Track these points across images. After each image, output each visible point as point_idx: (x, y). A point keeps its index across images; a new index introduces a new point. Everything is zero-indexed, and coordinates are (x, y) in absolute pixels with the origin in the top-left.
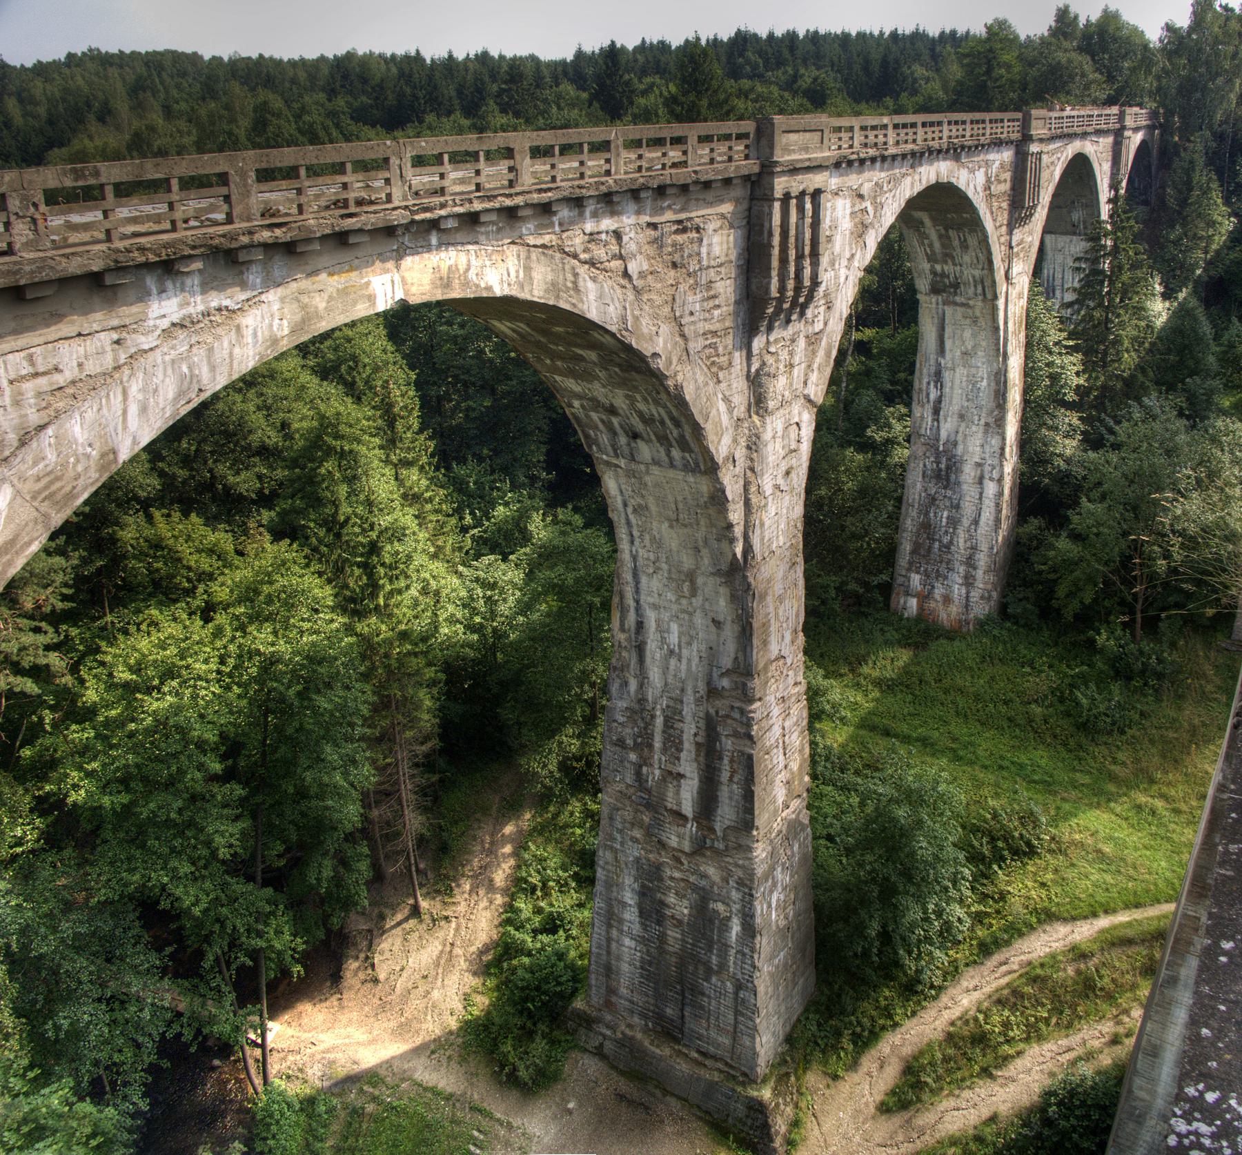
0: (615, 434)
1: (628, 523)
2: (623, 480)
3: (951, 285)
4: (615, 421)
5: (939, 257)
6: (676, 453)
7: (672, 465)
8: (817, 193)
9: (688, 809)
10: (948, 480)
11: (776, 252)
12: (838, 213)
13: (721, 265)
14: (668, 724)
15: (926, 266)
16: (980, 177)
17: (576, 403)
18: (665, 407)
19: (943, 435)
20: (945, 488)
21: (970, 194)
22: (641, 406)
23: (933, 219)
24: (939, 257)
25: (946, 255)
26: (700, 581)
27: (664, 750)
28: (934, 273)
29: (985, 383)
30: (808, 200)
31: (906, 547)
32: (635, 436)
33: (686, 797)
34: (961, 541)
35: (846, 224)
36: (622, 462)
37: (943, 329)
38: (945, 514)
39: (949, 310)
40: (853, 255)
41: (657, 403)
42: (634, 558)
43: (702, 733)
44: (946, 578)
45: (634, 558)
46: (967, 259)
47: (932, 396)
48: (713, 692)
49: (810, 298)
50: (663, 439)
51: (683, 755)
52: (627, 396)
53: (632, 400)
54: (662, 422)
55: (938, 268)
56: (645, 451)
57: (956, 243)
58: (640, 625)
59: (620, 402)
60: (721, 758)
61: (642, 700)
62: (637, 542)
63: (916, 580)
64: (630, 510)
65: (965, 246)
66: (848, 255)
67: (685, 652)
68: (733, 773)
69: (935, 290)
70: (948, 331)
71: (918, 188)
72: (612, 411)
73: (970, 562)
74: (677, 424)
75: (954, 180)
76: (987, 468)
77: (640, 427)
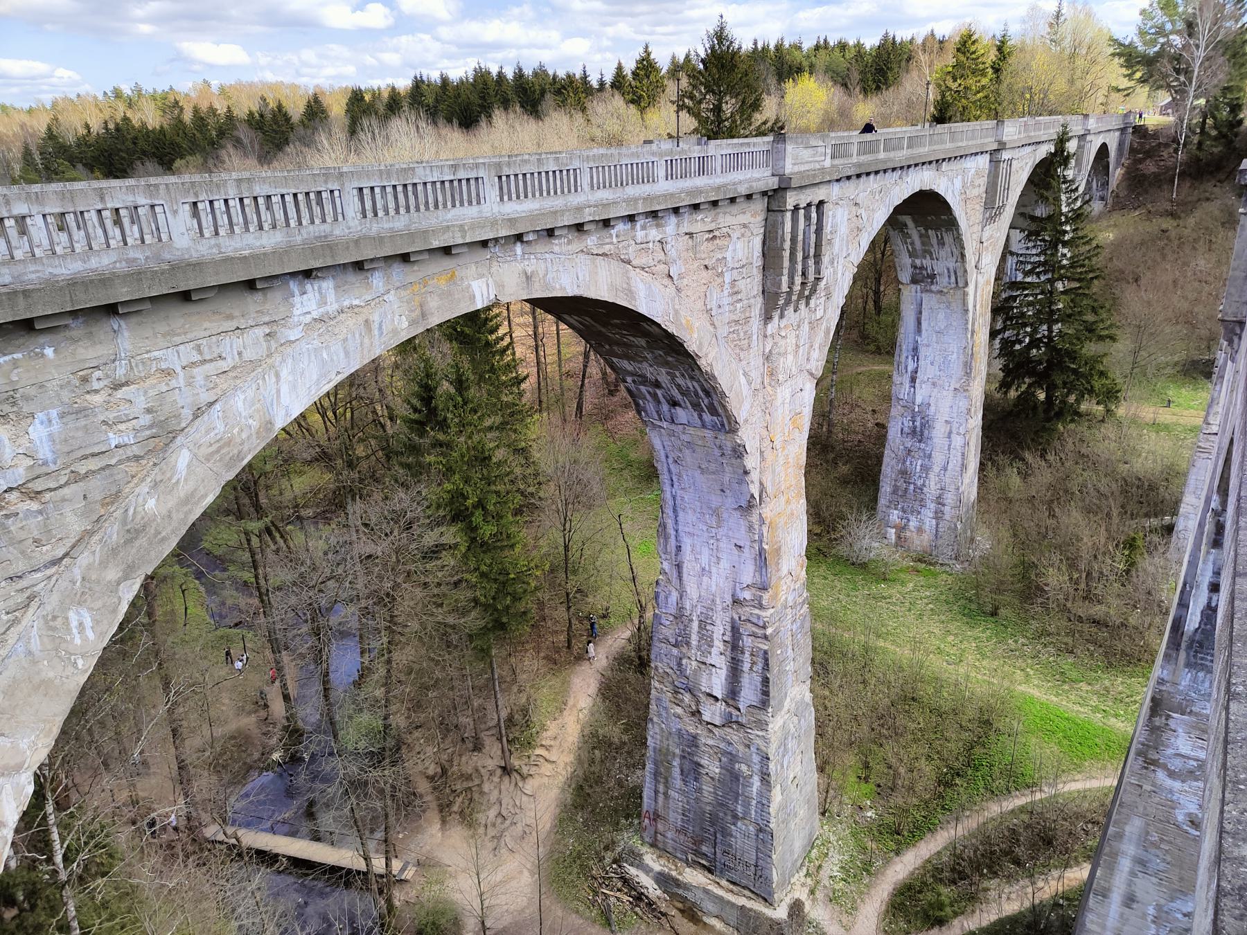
0: (659, 402)
1: (669, 471)
2: (666, 438)
3: (929, 276)
4: (659, 392)
5: (919, 253)
6: (707, 417)
7: (704, 426)
9: (718, 693)
10: (922, 435)
12: (838, 220)
14: (702, 624)
15: (906, 260)
17: (629, 379)
18: (698, 381)
19: (918, 400)
20: (920, 441)
22: (680, 381)
23: (914, 221)
24: (919, 253)
25: (925, 251)
26: (725, 515)
27: (699, 648)
29: (955, 356)
31: (886, 488)
32: (674, 404)
33: (717, 683)
34: (932, 483)
35: (843, 229)
36: (665, 425)
38: (919, 462)
41: (692, 378)
42: (674, 498)
43: (729, 633)
44: (919, 513)
45: (674, 498)
46: (943, 253)
47: (910, 368)
48: (736, 602)
49: (814, 291)
50: (696, 406)
51: (714, 651)
52: (668, 373)
53: (673, 377)
54: (696, 394)
55: (918, 262)
56: (682, 414)
58: (679, 548)
59: (664, 378)
60: (743, 653)
61: (681, 609)
62: (676, 484)
63: (895, 515)
64: (670, 460)
67: (714, 570)
68: (753, 663)
69: (914, 281)
72: (657, 385)
73: (939, 501)
74: (708, 394)
76: (955, 425)
77: (679, 397)
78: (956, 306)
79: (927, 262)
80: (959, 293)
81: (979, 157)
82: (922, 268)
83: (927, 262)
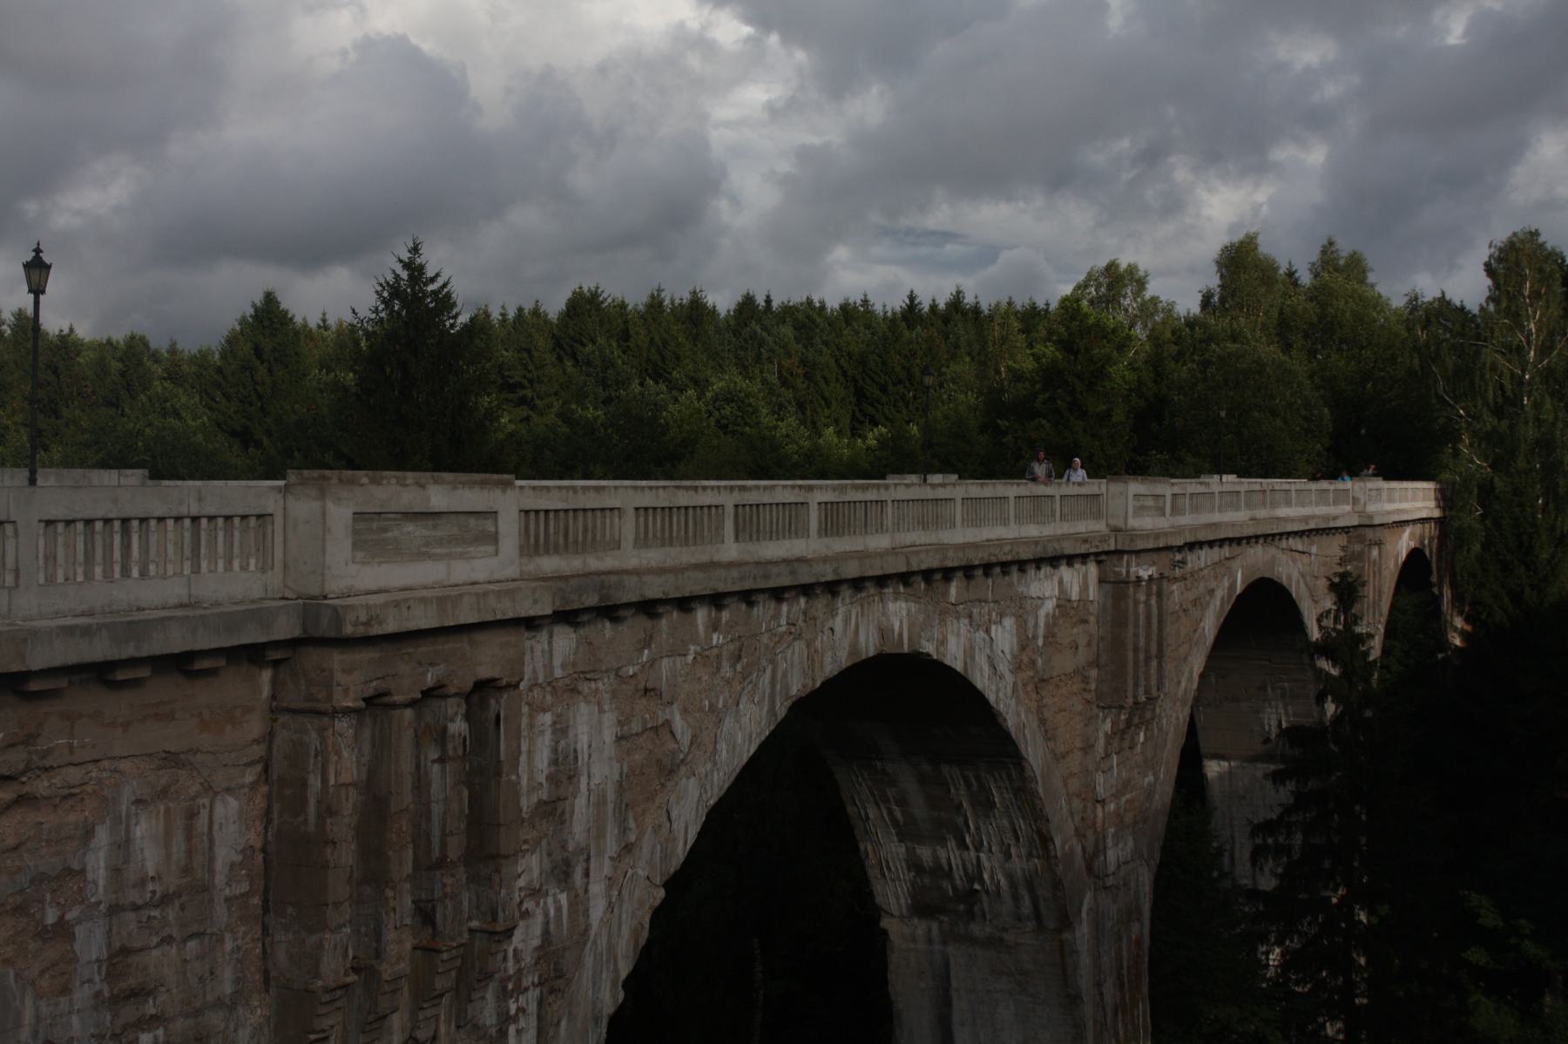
8: (485, 687)
11: (346, 856)
13: (165, 900)
16: (1004, 636)
21: (981, 680)
28: (915, 865)
30: (455, 707)
37: (948, 1002)
40: (628, 848)
55: (925, 853)
65: (985, 805)
66: (611, 847)
69: (922, 908)
70: (960, 1007)
71: (830, 666)
75: (929, 648)
79: (950, 854)
81: (1065, 572)
82: (941, 872)
83: (950, 854)
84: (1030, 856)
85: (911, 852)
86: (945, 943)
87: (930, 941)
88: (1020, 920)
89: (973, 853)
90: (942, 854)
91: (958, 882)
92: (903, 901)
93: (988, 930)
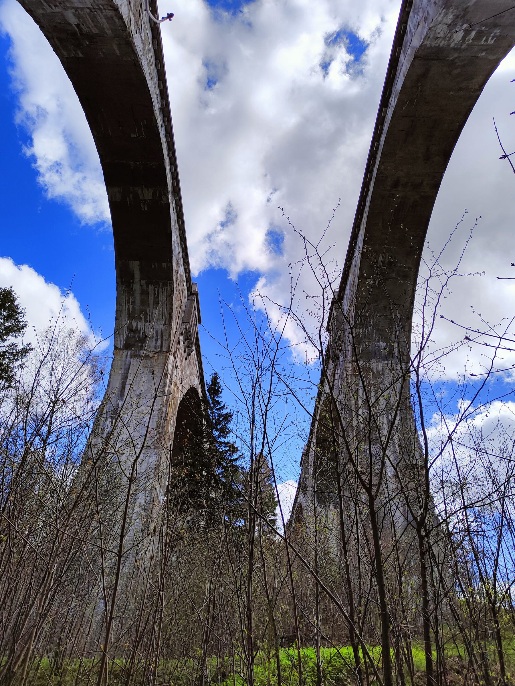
28: (130, 329)
37: (126, 377)
39: (134, 362)
55: (134, 324)
57: (151, 299)
78: (158, 371)
80: (162, 356)
82: (137, 331)
83: (141, 324)
84: (165, 324)
85: (130, 323)
86: (131, 357)
87: (127, 357)
88: (156, 348)
89: (148, 323)
90: (139, 324)
91: (141, 335)
92: (122, 343)
93: (145, 352)
